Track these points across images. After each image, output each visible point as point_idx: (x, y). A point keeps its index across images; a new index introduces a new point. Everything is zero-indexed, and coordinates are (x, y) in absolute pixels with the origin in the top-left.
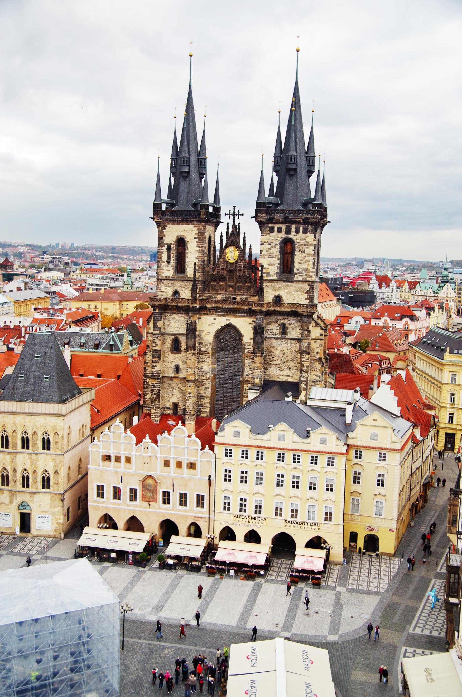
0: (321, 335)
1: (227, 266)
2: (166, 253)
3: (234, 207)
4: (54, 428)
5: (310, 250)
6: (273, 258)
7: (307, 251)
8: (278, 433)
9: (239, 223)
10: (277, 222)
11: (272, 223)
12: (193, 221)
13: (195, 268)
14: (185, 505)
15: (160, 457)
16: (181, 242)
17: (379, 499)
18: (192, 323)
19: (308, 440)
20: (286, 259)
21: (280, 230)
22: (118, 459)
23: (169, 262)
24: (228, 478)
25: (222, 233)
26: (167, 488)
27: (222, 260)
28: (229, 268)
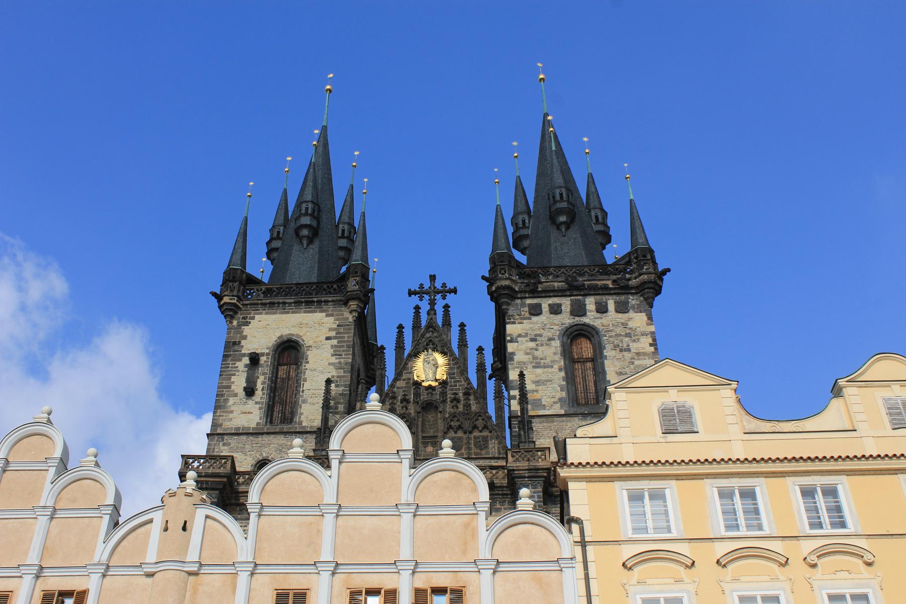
1: (417, 395)
2: (245, 375)
3: (433, 278)
5: (644, 344)
6: (545, 367)
7: (634, 347)
8: (880, 393)
9: (446, 307)
11: (534, 293)
12: (326, 302)
13: (328, 391)
16: (289, 351)
20: (579, 373)
21: (555, 310)
25: (400, 327)
27: (400, 384)
28: (424, 397)
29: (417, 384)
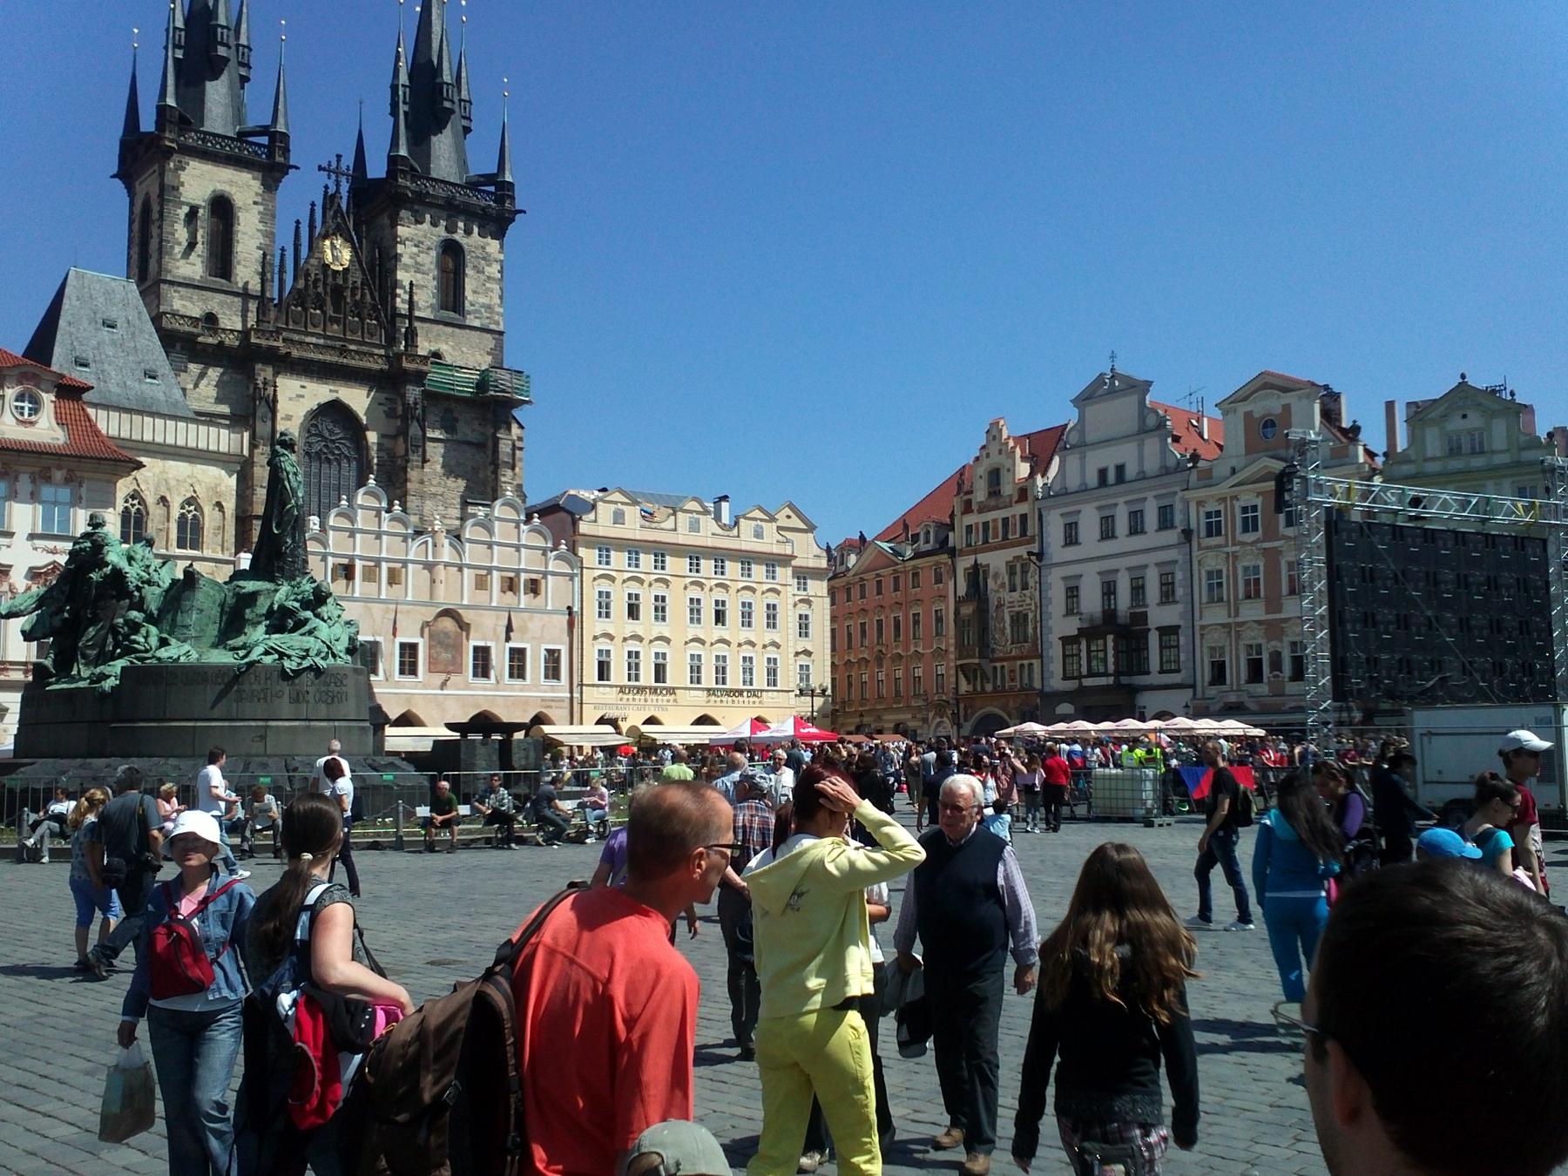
0: (520, 439)
1: (326, 277)
3: (339, 157)
4: (214, 489)
5: (493, 270)
10: (431, 205)
14: (522, 676)
15: (470, 567)
17: (803, 660)
18: (265, 383)
19: (735, 532)
22: (370, 575)
23: (192, 245)
24: (605, 611)
25: (313, 204)
26: (484, 639)
27: (313, 261)
29: (326, 267)
